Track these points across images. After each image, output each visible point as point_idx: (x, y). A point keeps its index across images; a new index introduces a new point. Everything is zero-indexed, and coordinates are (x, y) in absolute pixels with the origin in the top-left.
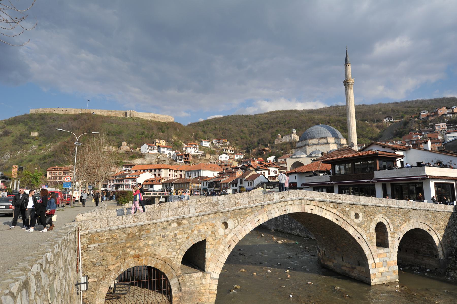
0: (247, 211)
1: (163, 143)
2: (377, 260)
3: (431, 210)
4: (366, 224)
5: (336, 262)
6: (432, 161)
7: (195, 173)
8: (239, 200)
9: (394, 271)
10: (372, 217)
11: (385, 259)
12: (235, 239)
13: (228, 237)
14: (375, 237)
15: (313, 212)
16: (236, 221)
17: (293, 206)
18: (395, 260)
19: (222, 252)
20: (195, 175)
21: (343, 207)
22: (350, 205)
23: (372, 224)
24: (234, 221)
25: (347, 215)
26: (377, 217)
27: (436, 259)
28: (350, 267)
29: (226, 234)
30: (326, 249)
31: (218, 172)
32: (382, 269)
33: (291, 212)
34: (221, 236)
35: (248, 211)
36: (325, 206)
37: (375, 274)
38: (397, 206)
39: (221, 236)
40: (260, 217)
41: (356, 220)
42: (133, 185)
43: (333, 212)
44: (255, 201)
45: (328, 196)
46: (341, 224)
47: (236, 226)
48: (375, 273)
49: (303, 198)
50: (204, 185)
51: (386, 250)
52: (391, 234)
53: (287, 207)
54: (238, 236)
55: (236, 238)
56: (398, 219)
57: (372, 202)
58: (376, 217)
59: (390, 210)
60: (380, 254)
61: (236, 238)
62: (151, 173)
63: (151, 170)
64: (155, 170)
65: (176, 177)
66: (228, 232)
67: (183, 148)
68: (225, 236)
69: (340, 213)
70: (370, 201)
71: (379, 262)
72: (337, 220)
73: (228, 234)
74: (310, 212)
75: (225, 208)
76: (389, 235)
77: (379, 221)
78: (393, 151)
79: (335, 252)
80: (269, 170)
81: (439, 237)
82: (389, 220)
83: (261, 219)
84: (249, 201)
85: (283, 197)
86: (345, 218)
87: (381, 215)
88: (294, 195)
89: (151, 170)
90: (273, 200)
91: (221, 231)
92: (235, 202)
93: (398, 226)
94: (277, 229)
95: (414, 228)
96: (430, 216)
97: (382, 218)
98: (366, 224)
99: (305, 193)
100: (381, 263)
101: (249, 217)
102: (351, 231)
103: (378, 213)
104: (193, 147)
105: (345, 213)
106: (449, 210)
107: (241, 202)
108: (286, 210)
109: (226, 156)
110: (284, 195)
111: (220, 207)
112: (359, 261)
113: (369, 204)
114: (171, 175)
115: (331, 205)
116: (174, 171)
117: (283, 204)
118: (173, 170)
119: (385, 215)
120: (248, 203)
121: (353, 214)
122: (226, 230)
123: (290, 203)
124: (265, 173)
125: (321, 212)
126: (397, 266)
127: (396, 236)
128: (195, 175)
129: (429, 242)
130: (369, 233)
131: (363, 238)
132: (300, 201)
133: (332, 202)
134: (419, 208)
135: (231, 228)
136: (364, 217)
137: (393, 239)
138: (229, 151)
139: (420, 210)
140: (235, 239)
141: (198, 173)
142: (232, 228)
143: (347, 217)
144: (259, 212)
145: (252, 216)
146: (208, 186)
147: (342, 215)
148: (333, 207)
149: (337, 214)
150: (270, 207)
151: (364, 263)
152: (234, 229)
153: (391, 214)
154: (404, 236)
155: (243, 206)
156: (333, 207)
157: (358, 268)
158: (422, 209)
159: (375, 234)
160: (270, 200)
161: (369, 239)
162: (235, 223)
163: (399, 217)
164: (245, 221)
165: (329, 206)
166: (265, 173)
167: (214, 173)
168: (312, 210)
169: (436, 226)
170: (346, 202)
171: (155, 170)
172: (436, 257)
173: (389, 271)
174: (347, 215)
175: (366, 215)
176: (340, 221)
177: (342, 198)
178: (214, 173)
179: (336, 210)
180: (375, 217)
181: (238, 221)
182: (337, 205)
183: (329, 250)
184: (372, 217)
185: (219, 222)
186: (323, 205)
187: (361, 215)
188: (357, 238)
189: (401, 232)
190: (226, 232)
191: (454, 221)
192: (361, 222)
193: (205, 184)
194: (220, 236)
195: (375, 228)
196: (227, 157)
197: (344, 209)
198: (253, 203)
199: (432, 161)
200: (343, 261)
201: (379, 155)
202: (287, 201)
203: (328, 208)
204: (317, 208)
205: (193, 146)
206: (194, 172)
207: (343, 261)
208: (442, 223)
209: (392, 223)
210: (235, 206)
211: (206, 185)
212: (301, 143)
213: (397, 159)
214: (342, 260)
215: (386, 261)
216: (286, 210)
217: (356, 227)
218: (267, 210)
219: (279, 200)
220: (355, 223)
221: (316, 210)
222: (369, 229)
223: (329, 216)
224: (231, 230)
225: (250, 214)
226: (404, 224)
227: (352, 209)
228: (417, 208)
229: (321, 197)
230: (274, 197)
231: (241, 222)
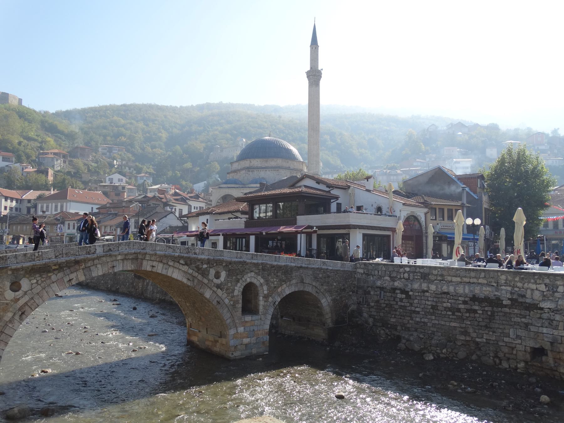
0: (51, 267)
2: (241, 329)
3: (322, 269)
4: (229, 285)
5: (200, 335)
6: (372, 205)
7: (56, 207)
8: (40, 253)
9: (263, 343)
10: (239, 277)
11: (252, 329)
12: (32, 304)
13: (20, 301)
14: (241, 301)
15: (154, 270)
16: (35, 281)
17: (125, 262)
18: (267, 329)
19: (11, 321)
20: (56, 210)
21: (199, 263)
22: (208, 262)
23: (239, 285)
24: (32, 281)
25: (205, 274)
26: (245, 277)
27: (324, 327)
28: (213, 340)
29: (18, 297)
30: (192, 320)
31: (98, 206)
32: (246, 341)
33: (121, 269)
34: (9, 300)
35: (54, 267)
36: (173, 262)
37: (236, 347)
38: (275, 263)
39: (9, 300)
40: (73, 276)
41: (215, 281)
43: (183, 270)
44: (66, 254)
45: (178, 249)
46: (194, 285)
47: (33, 287)
48: (237, 345)
49: (139, 251)
50: (69, 228)
51: (255, 317)
52: (263, 297)
53: (115, 263)
54: (37, 301)
55: (33, 303)
56: (275, 280)
57: (241, 258)
58: (245, 276)
59: (266, 267)
60: (246, 322)
61: (33, 303)
65: (20, 211)
66: (20, 296)
68: (16, 300)
69: (194, 272)
70: (239, 256)
71: (243, 331)
72: (189, 279)
73: (20, 298)
74: (149, 269)
75: (17, 263)
76: (261, 298)
77: (248, 280)
78: (327, 189)
79: (200, 323)
80: (190, 206)
81: (329, 301)
82: (262, 281)
83: (75, 278)
84: (57, 255)
85: (110, 249)
86: (200, 277)
87: (253, 274)
88: (127, 247)
90: (93, 253)
92: (34, 256)
93: (275, 287)
94: (164, 299)
95: (297, 290)
96: (321, 276)
97: (253, 278)
98: (229, 285)
99: (143, 246)
100: (246, 333)
101: (54, 275)
102: (208, 294)
103: (248, 271)
105: (199, 272)
106: (348, 268)
107: (44, 256)
108: (113, 267)
109: (121, 177)
110: (111, 248)
111: (9, 262)
112: (221, 332)
113: (236, 260)
115: (182, 262)
117: (109, 259)
118: (12, 199)
119: (258, 274)
120: (54, 257)
121: (212, 272)
122: (17, 293)
123: (119, 257)
124: (182, 210)
125: (167, 270)
126: (268, 337)
127: (270, 299)
128: (56, 210)
129: (318, 307)
130: (233, 297)
131: (224, 303)
132: (134, 255)
133: (182, 257)
134: (306, 266)
135: (25, 290)
136: (228, 276)
137: (266, 303)
138: (127, 168)
139: (307, 268)
140: (32, 304)
141: (62, 207)
142: (27, 290)
143: (202, 276)
144: (72, 269)
145: (60, 275)
146: (77, 229)
147: (197, 274)
148: (184, 263)
149: (189, 272)
150: (89, 264)
151: (226, 333)
152: (30, 291)
153: (266, 272)
154: (282, 300)
155: (47, 260)
156: (184, 263)
157: (220, 340)
158: (309, 266)
159: (242, 297)
160: (89, 253)
161: (232, 303)
162: (32, 284)
163: (277, 276)
164: (48, 282)
165: (178, 262)
166: (182, 210)
167: (92, 208)
168: (153, 266)
169: (327, 288)
170: (203, 257)
172: (324, 326)
173: (257, 343)
174: (205, 274)
175: (231, 273)
176: (193, 281)
177: (198, 252)
178: (92, 208)
179: (188, 268)
180: (243, 277)
181: (37, 281)
183: (194, 321)
184: (239, 277)
185: (6, 282)
186: (170, 260)
187: (223, 274)
188: (215, 303)
189: (279, 295)
190: (17, 296)
191: (351, 282)
192: (221, 283)
193: (71, 227)
194: (6, 300)
195: (242, 290)
196: (122, 179)
197: (201, 266)
198: (63, 257)
199: (372, 205)
200: (207, 333)
201: (303, 194)
202: (116, 256)
203: (177, 265)
204: (161, 265)
206: (54, 205)
207: (207, 333)
208: (335, 284)
209: (267, 284)
210: (34, 260)
211: (74, 228)
212: (237, 164)
213: (332, 201)
214: (206, 333)
215: (254, 330)
216: (113, 267)
217: (215, 289)
218: (83, 266)
219: (102, 254)
220: (214, 284)
221: (159, 267)
222: (234, 290)
223: (176, 275)
224: (25, 293)
225: (56, 272)
226: (283, 285)
227: (211, 266)
228: (303, 265)
229: (167, 251)
230: (96, 249)
231: (42, 282)
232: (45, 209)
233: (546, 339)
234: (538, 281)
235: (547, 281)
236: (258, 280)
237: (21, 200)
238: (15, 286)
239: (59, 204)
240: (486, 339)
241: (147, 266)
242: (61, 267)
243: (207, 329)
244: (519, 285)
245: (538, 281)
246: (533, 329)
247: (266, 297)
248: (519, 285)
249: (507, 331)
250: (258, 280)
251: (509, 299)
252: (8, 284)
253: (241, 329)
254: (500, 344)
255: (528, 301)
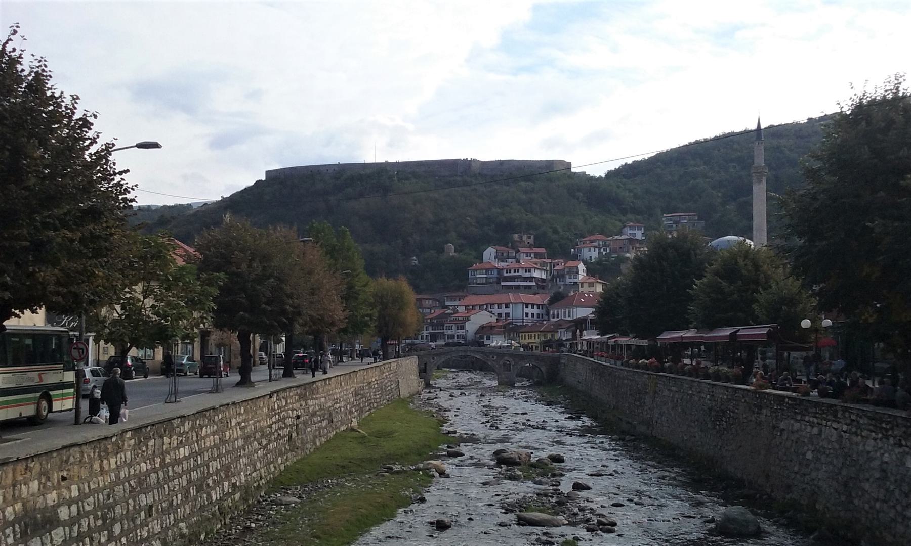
1: (529, 240)
32: (505, 380)
42: (458, 334)
62: (491, 312)
63: (492, 305)
64: (499, 306)
67: (572, 250)
89: (492, 305)
91: (432, 361)
104: (595, 247)
114: (530, 315)
116: (535, 307)
121: (491, 357)
136: (497, 358)
171: (499, 306)
182: (482, 353)
187: (495, 357)
205: (596, 244)
232: (567, 315)
236: (510, 360)
237: (542, 305)
238: (433, 359)
239: (567, 310)
241: (468, 354)
242: (444, 353)
247: (513, 365)
250: (510, 360)
252: (431, 358)
253: (503, 376)
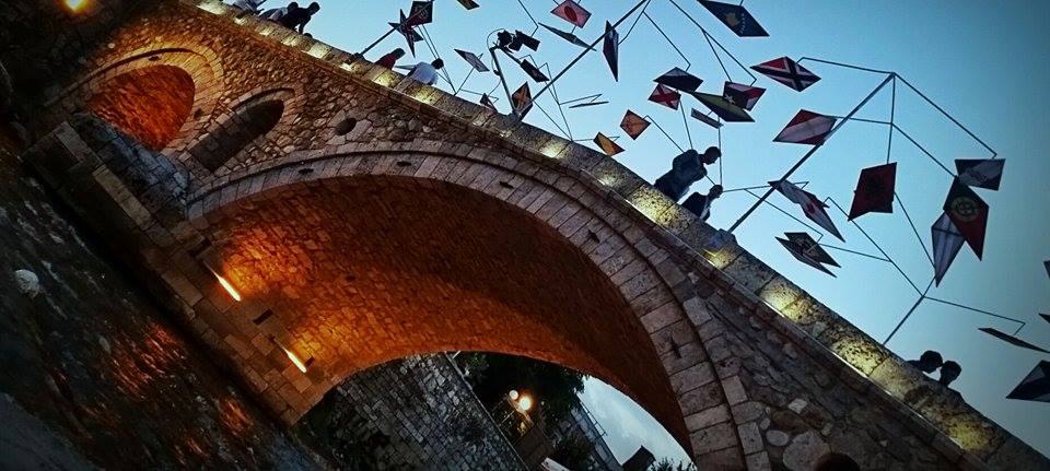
151: (326, 374)
200: (258, 321)
207: (258, 321)
233: (401, 434)
234: (445, 373)
235: (450, 378)
240: (349, 395)
243: (267, 314)
244: (430, 362)
245: (445, 373)
246: (399, 415)
248: (430, 362)
249: (375, 400)
251: (408, 369)
254: (357, 408)
255: (420, 384)
